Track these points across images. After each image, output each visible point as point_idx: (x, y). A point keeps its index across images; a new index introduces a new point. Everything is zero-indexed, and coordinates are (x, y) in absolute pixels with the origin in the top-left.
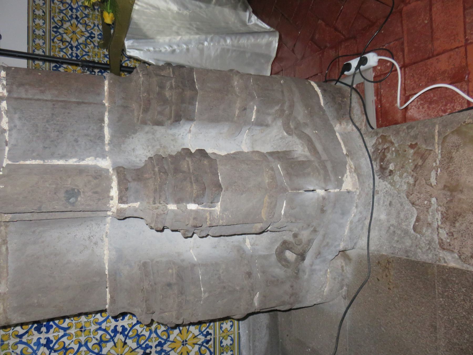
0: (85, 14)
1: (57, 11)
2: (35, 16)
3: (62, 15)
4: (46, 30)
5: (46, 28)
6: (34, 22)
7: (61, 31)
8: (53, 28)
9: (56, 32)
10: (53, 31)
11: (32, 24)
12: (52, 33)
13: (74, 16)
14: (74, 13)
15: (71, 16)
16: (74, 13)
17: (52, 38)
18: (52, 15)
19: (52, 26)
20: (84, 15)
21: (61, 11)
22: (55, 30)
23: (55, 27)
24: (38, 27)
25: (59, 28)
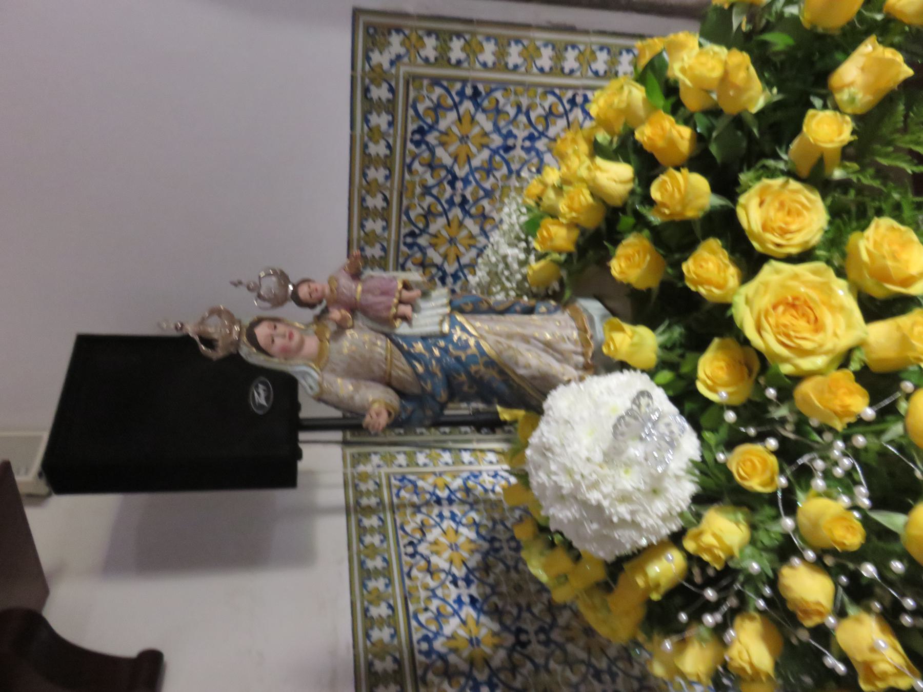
0: (484, 190)
1: (418, 190)
2: (366, 213)
3: (429, 200)
4: (389, 244)
5: (388, 241)
6: (362, 226)
7: (423, 241)
8: (406, 236)
9: (410, 246)
10: (405, 244)
11: (359, 234)
12: (404, 248)
13: (457, 199)
14: (459, 192)
15: (451, 202)
16: (459, 192)
17: (401, 260)
18: (405, 202)
19: (404, 231)
20: (481, 193)
21: (427, 191)
22: (409, 240)
23: (412, 234)
24: (371, 238)
25: (420, 235)
